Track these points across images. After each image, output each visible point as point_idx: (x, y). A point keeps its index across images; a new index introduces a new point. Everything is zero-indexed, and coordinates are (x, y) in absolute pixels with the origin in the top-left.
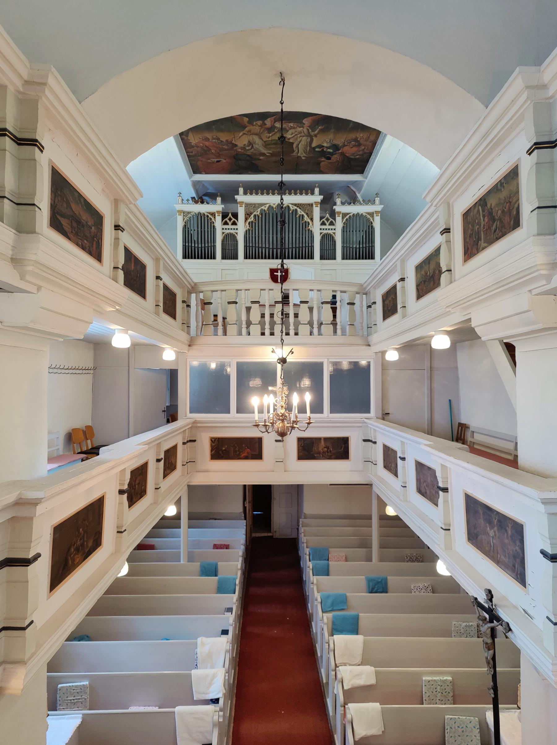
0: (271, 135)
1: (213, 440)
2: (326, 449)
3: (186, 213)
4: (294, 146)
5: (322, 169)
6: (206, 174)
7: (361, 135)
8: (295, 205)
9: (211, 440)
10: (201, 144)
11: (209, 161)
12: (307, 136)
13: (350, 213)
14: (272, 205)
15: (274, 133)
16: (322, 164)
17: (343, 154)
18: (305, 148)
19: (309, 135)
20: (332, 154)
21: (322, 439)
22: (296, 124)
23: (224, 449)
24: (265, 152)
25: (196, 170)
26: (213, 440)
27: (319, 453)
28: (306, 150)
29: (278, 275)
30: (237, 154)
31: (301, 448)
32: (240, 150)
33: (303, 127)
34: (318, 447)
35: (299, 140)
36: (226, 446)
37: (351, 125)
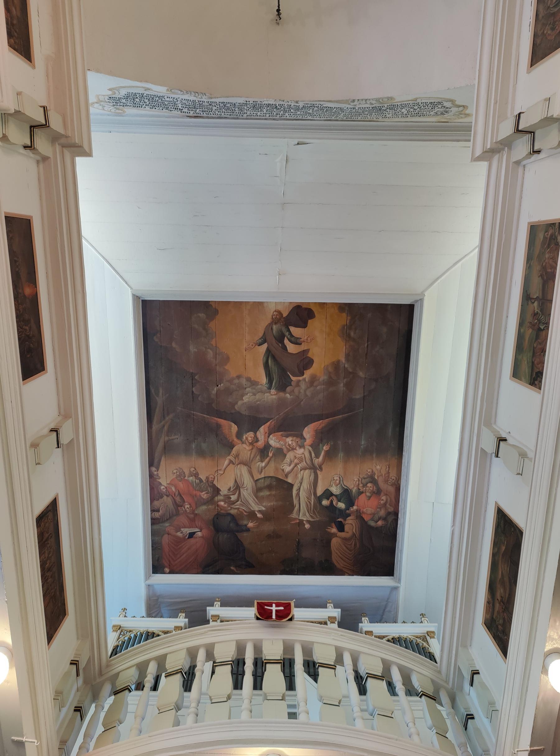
0: (263, 464)
3: (125, 632)
4: (294, 492)
5: (335, 558)
6: (170, 573)
7: (378, 467)
10: (173, 489)
11: (179, 534)
12: (310, 469)
15: (268, 459)
17: (359, 516)
18: (309, 498)
19: (314, 468)
20: (344, 514)
22: (295, 438)
24: (255, 507)
28: (310, 503)
29: (272, 610)
30: (218, 516)
35: (300, 476)
37: (363, 443)
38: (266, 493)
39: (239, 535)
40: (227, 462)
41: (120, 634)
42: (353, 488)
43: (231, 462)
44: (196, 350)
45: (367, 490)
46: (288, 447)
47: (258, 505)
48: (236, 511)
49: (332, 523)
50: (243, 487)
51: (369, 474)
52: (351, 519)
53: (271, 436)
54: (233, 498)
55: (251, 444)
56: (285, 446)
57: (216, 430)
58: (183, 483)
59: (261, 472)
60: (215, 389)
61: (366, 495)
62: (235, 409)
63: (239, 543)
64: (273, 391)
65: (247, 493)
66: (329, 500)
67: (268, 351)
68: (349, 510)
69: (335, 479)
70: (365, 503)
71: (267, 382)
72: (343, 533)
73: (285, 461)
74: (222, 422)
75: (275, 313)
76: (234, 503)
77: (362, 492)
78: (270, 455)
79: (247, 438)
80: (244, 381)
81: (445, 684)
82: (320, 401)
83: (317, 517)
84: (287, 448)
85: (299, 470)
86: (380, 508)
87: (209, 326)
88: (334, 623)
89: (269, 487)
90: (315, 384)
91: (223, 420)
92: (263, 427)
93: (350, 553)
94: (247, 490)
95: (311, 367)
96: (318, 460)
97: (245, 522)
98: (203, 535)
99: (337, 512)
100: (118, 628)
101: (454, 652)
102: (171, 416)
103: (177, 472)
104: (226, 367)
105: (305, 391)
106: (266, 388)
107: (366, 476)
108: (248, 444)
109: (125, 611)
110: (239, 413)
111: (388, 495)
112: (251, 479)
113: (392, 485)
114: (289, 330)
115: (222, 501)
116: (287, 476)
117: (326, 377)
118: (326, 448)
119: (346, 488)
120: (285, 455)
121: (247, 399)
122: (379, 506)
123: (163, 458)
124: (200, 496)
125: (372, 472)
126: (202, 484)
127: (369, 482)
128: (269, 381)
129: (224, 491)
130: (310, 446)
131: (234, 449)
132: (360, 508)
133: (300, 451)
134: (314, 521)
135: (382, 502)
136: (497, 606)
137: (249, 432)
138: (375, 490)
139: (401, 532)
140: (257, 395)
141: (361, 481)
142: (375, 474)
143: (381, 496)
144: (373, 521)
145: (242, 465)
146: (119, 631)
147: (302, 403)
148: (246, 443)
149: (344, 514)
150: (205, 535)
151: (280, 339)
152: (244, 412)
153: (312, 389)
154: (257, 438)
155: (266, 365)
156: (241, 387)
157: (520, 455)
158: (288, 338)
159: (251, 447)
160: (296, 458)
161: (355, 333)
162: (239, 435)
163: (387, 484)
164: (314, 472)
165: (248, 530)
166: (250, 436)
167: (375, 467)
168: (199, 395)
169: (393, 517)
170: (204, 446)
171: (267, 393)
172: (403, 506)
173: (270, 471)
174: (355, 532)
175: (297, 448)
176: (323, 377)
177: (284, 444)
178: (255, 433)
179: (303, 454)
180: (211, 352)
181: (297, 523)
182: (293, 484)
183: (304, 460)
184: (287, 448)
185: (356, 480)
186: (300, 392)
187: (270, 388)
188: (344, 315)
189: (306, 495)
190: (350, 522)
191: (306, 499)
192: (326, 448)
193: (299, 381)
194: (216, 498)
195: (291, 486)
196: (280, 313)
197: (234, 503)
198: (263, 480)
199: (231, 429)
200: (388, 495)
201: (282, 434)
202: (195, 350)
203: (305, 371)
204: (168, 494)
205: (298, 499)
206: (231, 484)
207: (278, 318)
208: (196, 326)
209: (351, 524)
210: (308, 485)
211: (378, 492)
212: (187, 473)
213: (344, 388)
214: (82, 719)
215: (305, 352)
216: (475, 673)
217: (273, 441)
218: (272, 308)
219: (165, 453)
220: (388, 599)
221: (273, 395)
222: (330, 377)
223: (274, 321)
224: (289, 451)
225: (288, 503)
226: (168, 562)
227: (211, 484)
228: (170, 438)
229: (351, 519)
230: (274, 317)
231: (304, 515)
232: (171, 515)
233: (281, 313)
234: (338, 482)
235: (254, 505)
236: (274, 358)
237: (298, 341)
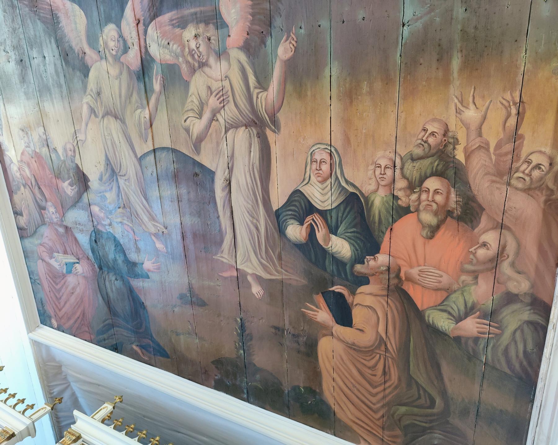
18: (253, 216)
22: (202, 26)
28: (257, 229)
42: (376, 191)
45: (424, 204)
49: (318, 294)
50: (121, 174)
51: (431, 140)
52: (370, 294)
55: (117, 59)
56: (183, 56)
61: (419, 220)
66: (305, 225)
68: (363, 263)
69: (318, 157)
72: (348, 329)
73: (188, 106)
84: (187, 62)
85: (224, 130)
86: (475, 275)
93: (374, 391)
96: (265, 94)
99: (330, 267)
107: (419, 151)
108: (110, 59)
111: (508, 229)
113: (527, 190)
119: (351, 189)
120: (187, 85)
122: (468, 267)
125: (444, 135)
127: (433, 174)
130: (240, 48)
132: (401, 262)
134: (270, 280)
138: (452, 204)
141: (402, 169)
142: (456, 141)
143: (476, 230)
144: (445, 315)
160: (211, 94)
163: (509, 184)
167: (458, 112)
169: (526, 315)
174: (384, 336)
175: (212, 61)
177: (179, 50)
178: (119, 26)
179: (226, 77)
181: (234, 277)
183: (231, 98)
184: (187, 62)
185: (383, 162)
189: (245, 203)
190: (369, 301)
191: (248, 218)
192: (286, 51)
200: (508, 229)
201: (171, 20)
210: (248, 176)
224: (193, 71)
229: (370, 294)
234: (325, 168)
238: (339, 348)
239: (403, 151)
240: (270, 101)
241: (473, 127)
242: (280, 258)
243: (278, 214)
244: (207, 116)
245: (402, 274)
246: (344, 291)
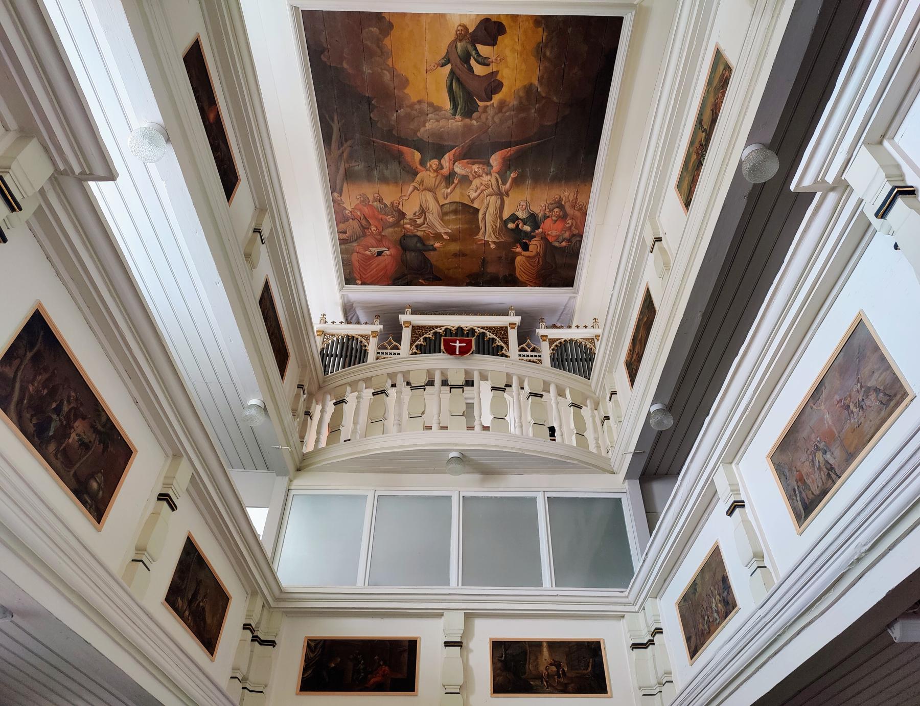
0: (449, 191)
1: (313, 644)
2: (554, 668)
3: (328, 336)
4: (480, 216)
5: (518, 273)
6: (362, 284)
8: (483, 328)
9: (308, 645)
11: (367, 252)
12: (497, 195)
13: (560, 339)
14: (450, 327)
15: (453, 185)
16: (518, 259)
17: (544, 238)
19: (501, 195)
20: (530, 236)
21: (545, 644)
22: (481, 165)
23: (333, 665)
24: (441, 230)
25: (349, 280)
26: (313, 644)
27: (540, 677)
31: (499, 665)
32: (408, 226)
33: (490, 174)
34: (537, 664)
35: (486, 202)
36: (339, 660)
38: (452, 217)
39: (427, 254)
40: (411, 189)
41: (324, 338)
43: (415, 188)
44: (371, 72)
46: (474, 174)
47: (444, 227)
48: (422, 233)
53: (456, 163)
54: (419, 221)
55: (435, 171)
56: (471, 173)
57: (398, 157)
58: (367, 208)
59: (447, 197)
60: (395, 115)
61: (552, 219)
62: (418, 137)
63: (426, 260)
64: (458, 117)
65: (433, 217)
67: (452, 72)
69: (522, 204)
70: (550, 225)
71: (452, 107)
72: (527, 252)
74: (404, 149)
75: (459, 28)
76: (420, 226)
77: (549, 217)
78: (456, 182)
79: (431, 166)
80: (425, 107)
81: (593, 395)
82: (509, 128)
83: (502, 238)
87: (383, 43)
88: (514, 328)
89: (455, 212)
90: (504, 110)
91: (405, 148)
92: (447, 154)
94: (432, 214)
95: (500, 91)
97: (432, 243)
98: (391, 253)
99: (522, 234)
100: (322, 333)
101: (602, 375)
102: (349, 143)
103: (360, 198)
104: (406, 91)
105: (493, 118)
106: (450, 114)
108: (432, 171)
109: (325, 316)
110: (421, 140)
112: (437, 205)
114: (476, 49)
115: (408, 224)
116: (472, 201)
117: (516, 103)
118: (513, 175)
119: (532, 212)
121: (430, 126)
123: (345, 185)
124: (386, 220)
126: (387, 208)
127: (556, 208)
128: (453, 105)
129: (409, 215)
131: (418, 176)
133: (486, 178)
135: (567, 225)
136: (635, 355)
137: (433, 159)
138: (561, 215)
139: (584, 251)
140: (440, 122)
145: (427, 191)
146: (323, 336)
147: (489, 130)
148: (430, 170)
149: (530, 236)
150: (392, 253)
151: (466, 58)
152: (426, 138)
153: (500, 115)
154: (442, 166)
155: (450, 89)
156: (422, 113)
157: (664, 264)
158: (474, 58)
159: (435, 174)
161: (551, 52)
162: (423, 163)
164: (500, 198)
165: (435, 249)
166: (434, 163)
168: (378, 121)
170: (387, 173)
171: (451, 119)
172: (588, 229)
173: (456, 197)
175: (484, 175)
176: (514, 102)
177: (470, 171)
178: (440, 160)
180: (387, 73)
182: (479, 208)
184: (473, 175)
186: (487, 119)
187: (454, 114)
188: (540, 30)
190: (535, 242)
191: (492, 223)
192: (513, 175)
193: (487, 107)
194: (402, 221)
195: (477, 211)
196: (465, 28)
197: (420, 226)
198: (448, 206)
199: (414, 157)
201: (468, 162)
202: (369, 71)
203: (493, 96)
204: (353, 218)
205: (484, 222)
206: (417, 209)
207: (463, 34)
208: (369, 43)
209: (535, 245)
210: (494, 211)
211: (564, 217)
212: (371, 198)
213: (536, 114)
214: (311, 419)
215: (494, 74)
216: (614, 393)
217: (459, 169)
218: (455, 24)
219: (347, 179)
220: (566, 304)
221: (458, 122)
222: (521, 103)
223: (459, 38)
224: (475, 178)
225: (474, 226)
226: (359, 275)
227: (396, 209)
228: (351, 165)
230: (458, 33)
231: (490, 236)
232: (358, 236)
233: (467, 28)
234: (524, 207)
235: (440, 227)
236: (458, 80)
237: (486, 61)
238: (523, 258)
239: (548, 202)
240: (506, 189)
241: (567, 197)
242: (504, 234)
243: (505, 221)
244: (479, 192)
245: (546, 234)
246: (527, 241)
